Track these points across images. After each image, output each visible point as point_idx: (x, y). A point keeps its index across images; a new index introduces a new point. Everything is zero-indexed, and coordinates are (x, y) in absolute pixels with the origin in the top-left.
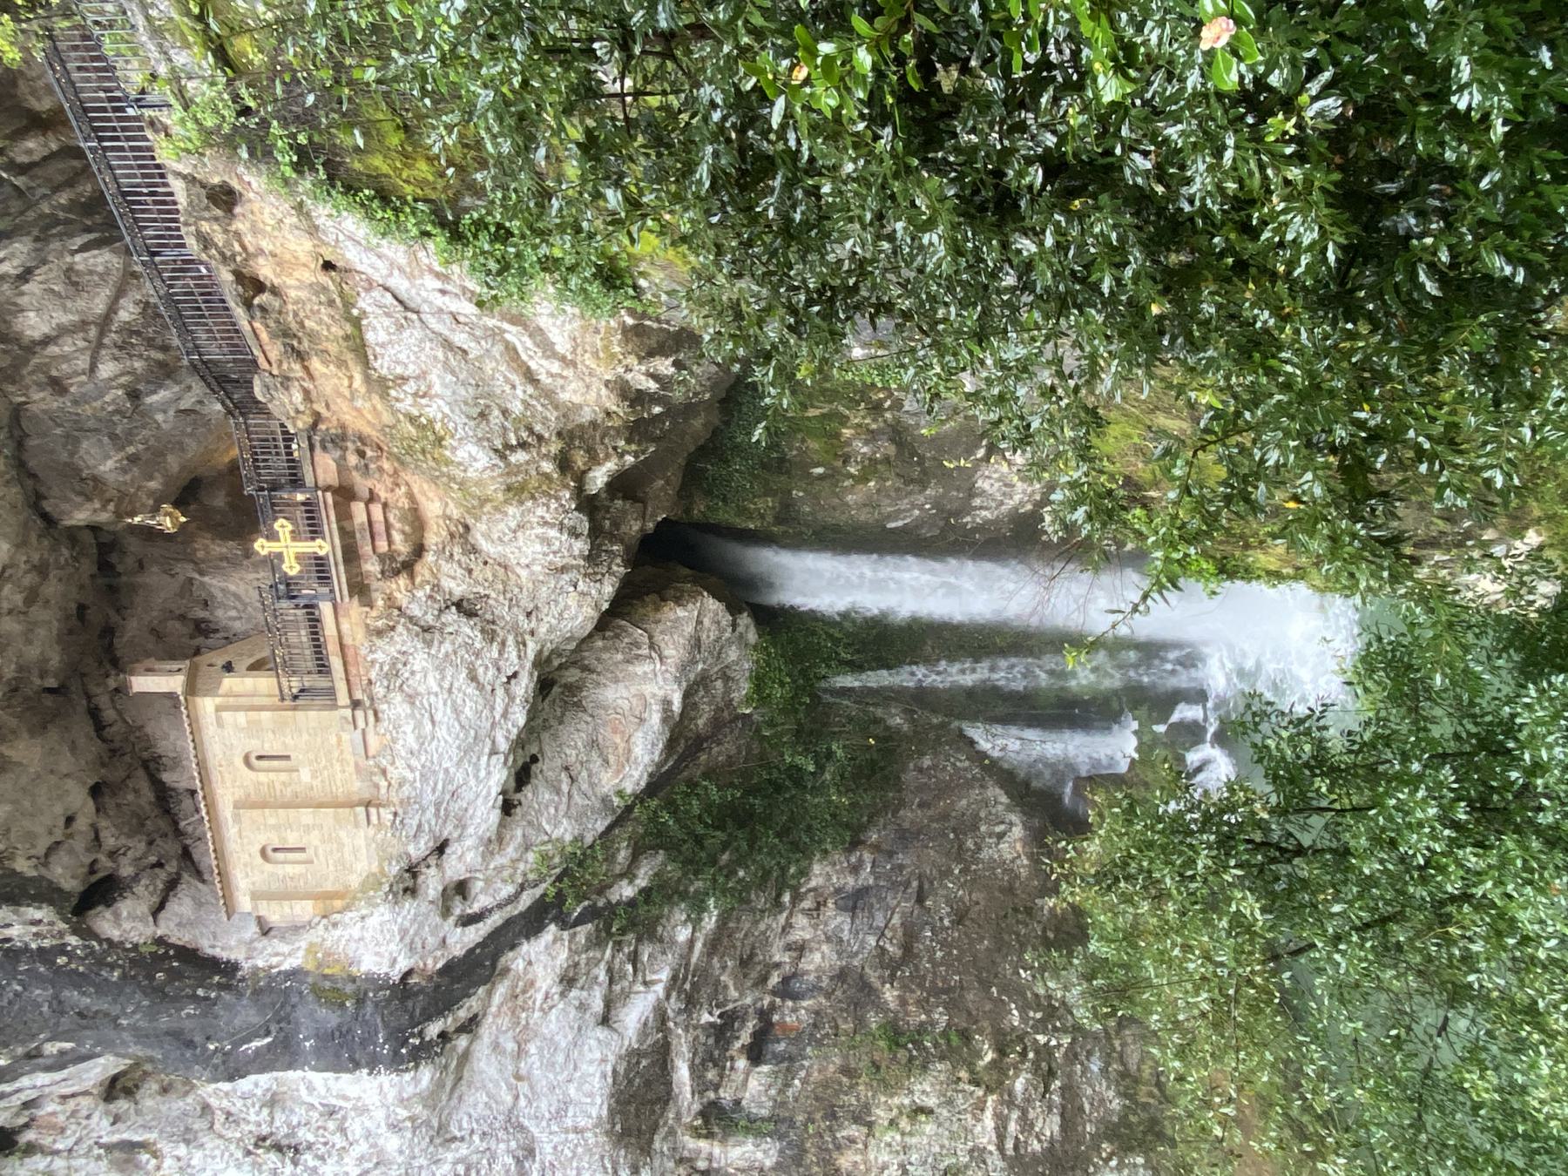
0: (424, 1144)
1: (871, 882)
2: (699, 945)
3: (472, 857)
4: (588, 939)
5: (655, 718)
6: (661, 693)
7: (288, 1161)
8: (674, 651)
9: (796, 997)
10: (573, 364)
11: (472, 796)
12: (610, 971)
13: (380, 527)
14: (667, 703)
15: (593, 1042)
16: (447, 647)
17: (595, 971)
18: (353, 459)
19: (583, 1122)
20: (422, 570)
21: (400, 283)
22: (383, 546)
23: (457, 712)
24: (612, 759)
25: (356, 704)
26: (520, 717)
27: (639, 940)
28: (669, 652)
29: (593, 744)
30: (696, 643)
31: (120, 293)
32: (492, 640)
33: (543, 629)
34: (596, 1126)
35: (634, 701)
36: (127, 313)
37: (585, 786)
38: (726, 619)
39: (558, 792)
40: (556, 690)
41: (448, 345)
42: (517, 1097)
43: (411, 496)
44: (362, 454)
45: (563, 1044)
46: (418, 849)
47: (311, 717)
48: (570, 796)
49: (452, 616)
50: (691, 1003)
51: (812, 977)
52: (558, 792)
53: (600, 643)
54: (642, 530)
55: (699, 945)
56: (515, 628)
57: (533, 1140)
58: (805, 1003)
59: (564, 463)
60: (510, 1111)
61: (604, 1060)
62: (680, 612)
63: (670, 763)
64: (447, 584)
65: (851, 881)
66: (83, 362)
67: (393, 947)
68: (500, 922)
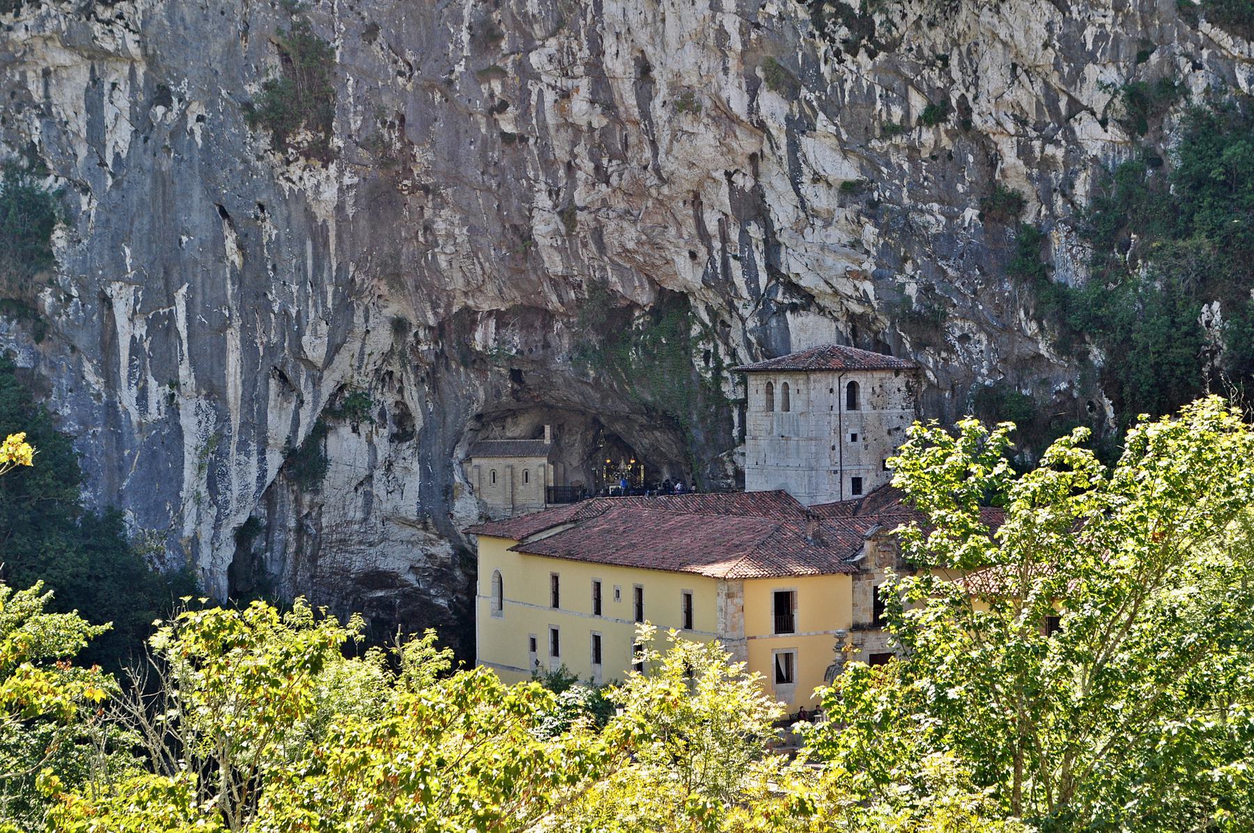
47: (542, 494)
50: (405, 596)
67: (463, 514)
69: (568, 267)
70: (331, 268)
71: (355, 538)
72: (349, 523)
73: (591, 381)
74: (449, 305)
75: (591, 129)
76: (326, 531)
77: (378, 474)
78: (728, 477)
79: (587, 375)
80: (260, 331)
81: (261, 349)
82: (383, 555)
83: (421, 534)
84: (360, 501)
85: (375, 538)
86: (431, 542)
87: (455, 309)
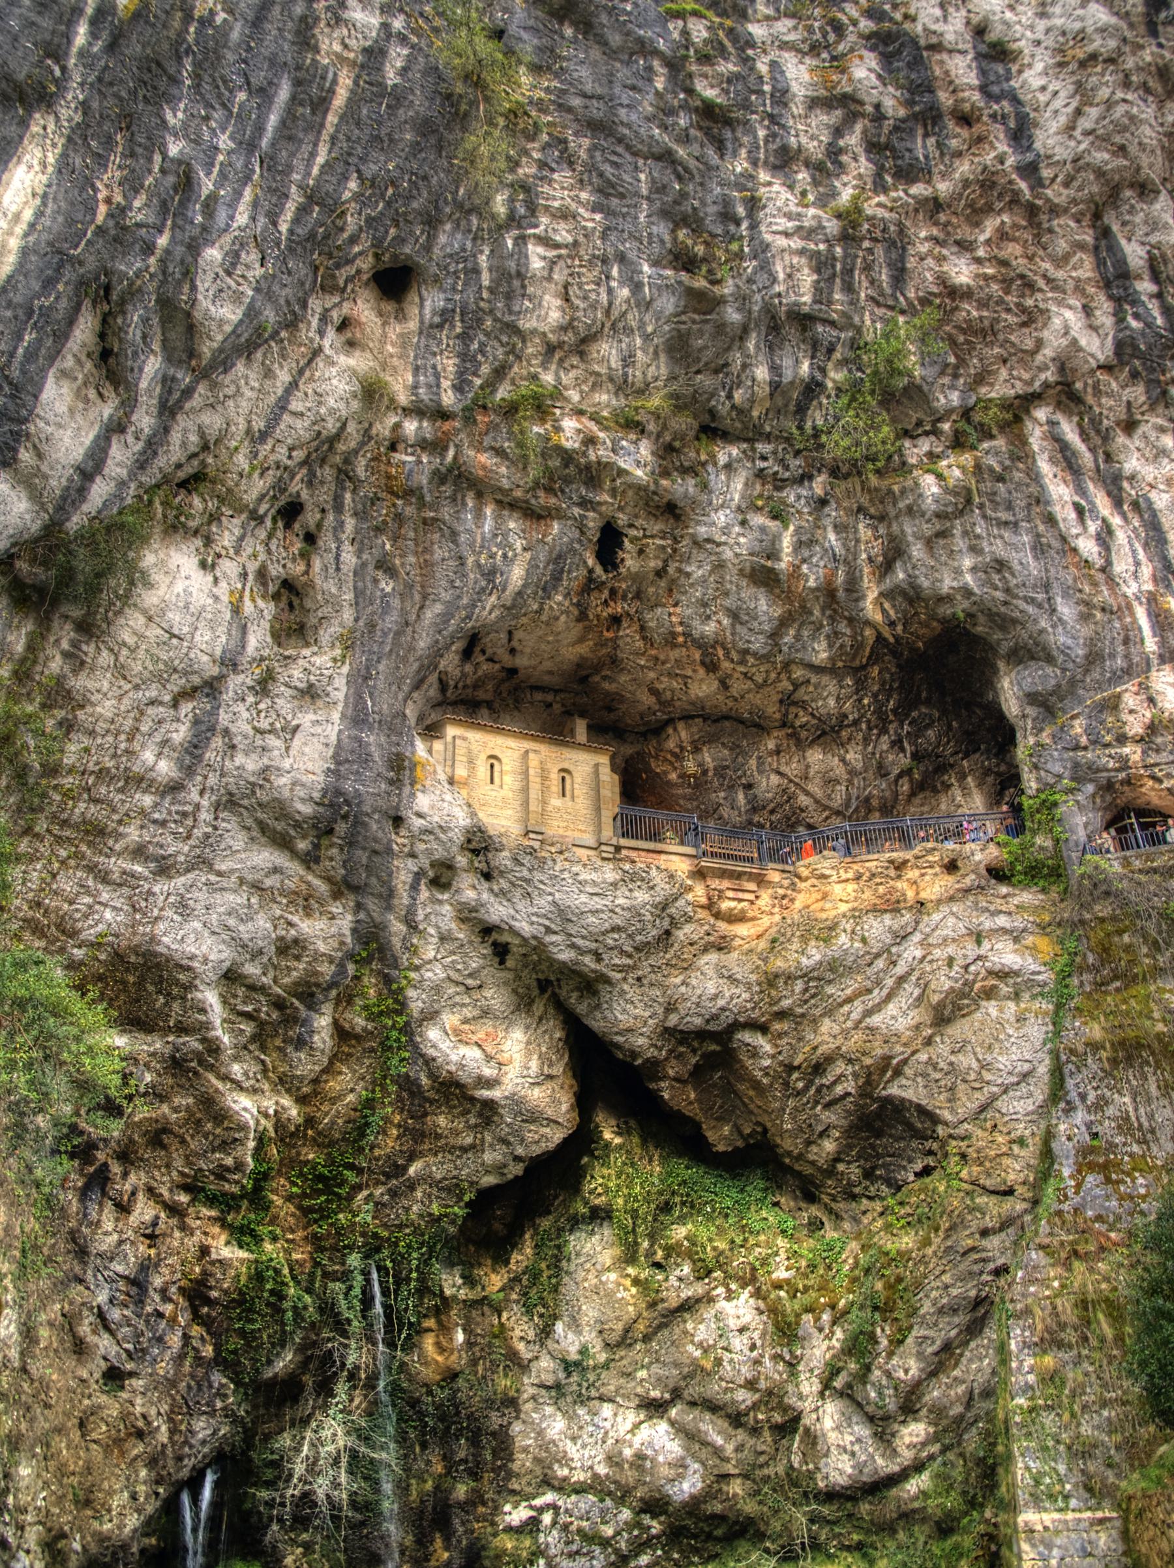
0: (231, 787)
1: (149, 1309)
2: (219, 1085)
3: (470, 894)
4: (316, 973)
5: (488, 1072)
6: (506, 1080)
7: (249, 682)
8: (537, 1096)
9: (84, 1194)
10: (856, 1027)
11: (519, 907)
12: (263, 989)
13: (741, 895)
14: (490, 1083)
15: (224, 956)
16: (649, 917)
17: (271, 974)
18: (781, 891)
19: (162, 926)
20: (702, 914)
21: (917, 937)
22: (730, 894)
23: (595, 912)
24: (466, 1027)
25: (618, 849)
26: (565, 956)
27: (262, 1025)
28: (536, 1093)
29: (485, 1013)
30: (534, 1117)
31: (817, 801)
32: (637, 949)
33: (626, 987)
34: (153, 939)
35: (506, 1055)
36: (803, 800)
37: (457, 999)
38: (536, 1150)
39: (470, 975)
40: (536, 992)
41: (878, 956)
42: (220, 874)
43: (754, 919)
44: (784, 897)
45: (242, 928)
46: (503, 859)
48: (457, 983)
49: (666, 924)
51: (94, 1216)
52: (470, 975)
53: (558, 1035)
54: (665, 1077)
55: (219, 1085)
56: (634, 967)
57: (170, 878)
58: (75, 1202)
59: (782, 1015)
60: (211, 866)
61: (206, 961)
62: (564, 1107)
63: (424, 1081)
64: (688, 928)
65: (158, 1281)
66: (783, 769)
68: (396, 901)
69: (821, 294)
70: (313, 155)
71: (133, 834)
72: (139, 781)
73: (783, 565)
74: (500, 372)
75: (879, 115)
76: (68, 781)
77: (236, 682)
78: (1122, 739)
79: (773, 554)
80: (113, 173)
81: (102, 209)
82: (183, 908)
83: (294, 868)
84: (181, 733)
85: (179, 849)
86: (306, 902)
87: (503, 392)
